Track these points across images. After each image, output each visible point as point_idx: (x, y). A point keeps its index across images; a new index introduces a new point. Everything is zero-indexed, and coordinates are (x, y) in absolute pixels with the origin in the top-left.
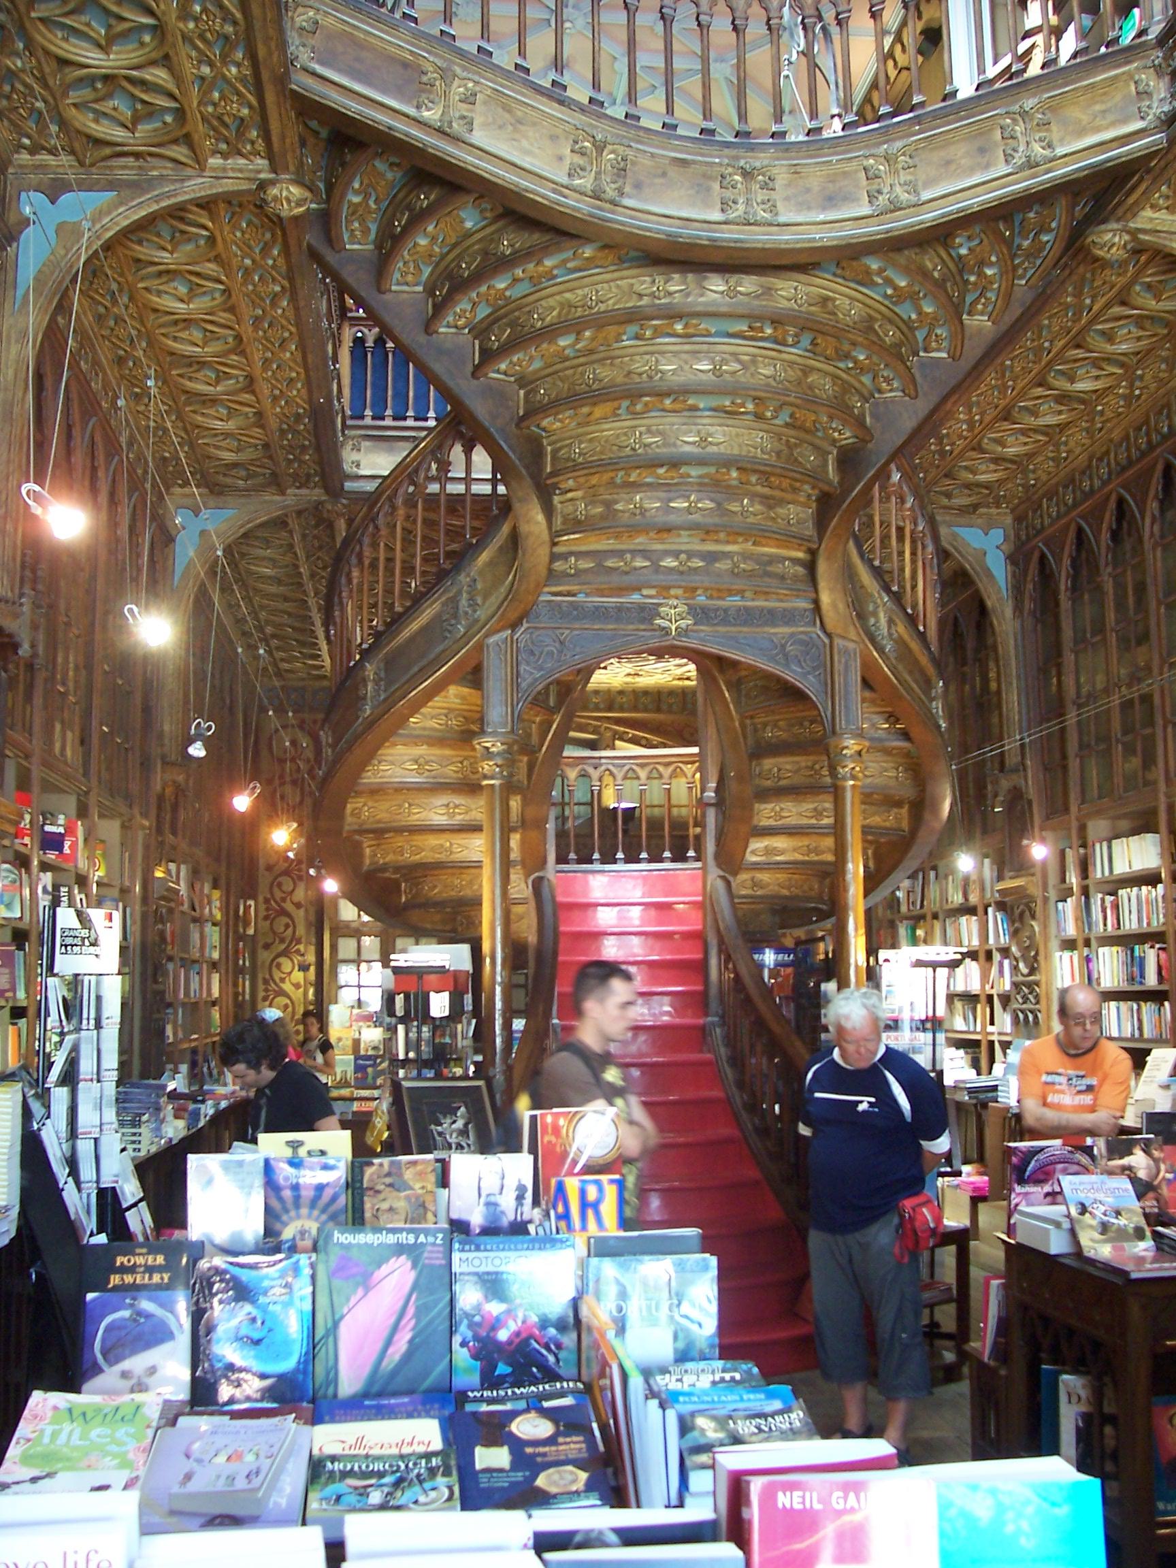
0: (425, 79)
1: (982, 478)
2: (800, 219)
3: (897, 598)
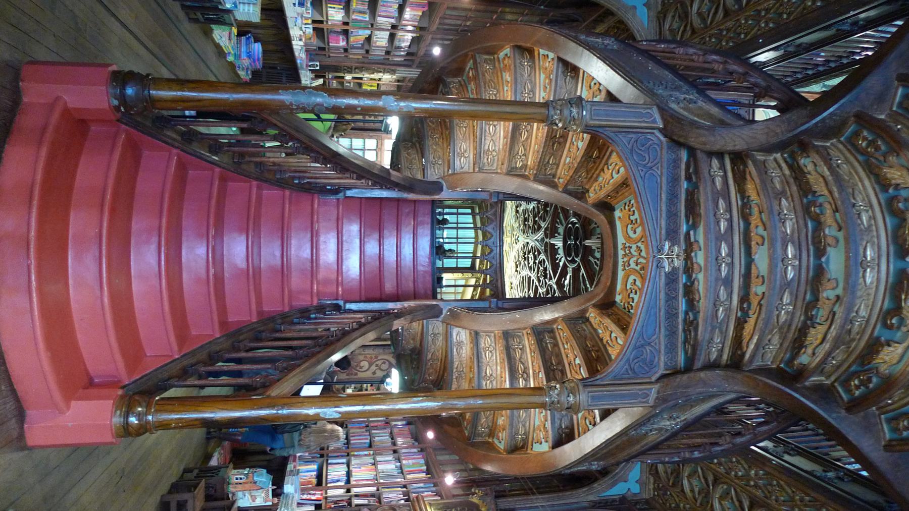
1: (685, 482)
3: (674, 435)
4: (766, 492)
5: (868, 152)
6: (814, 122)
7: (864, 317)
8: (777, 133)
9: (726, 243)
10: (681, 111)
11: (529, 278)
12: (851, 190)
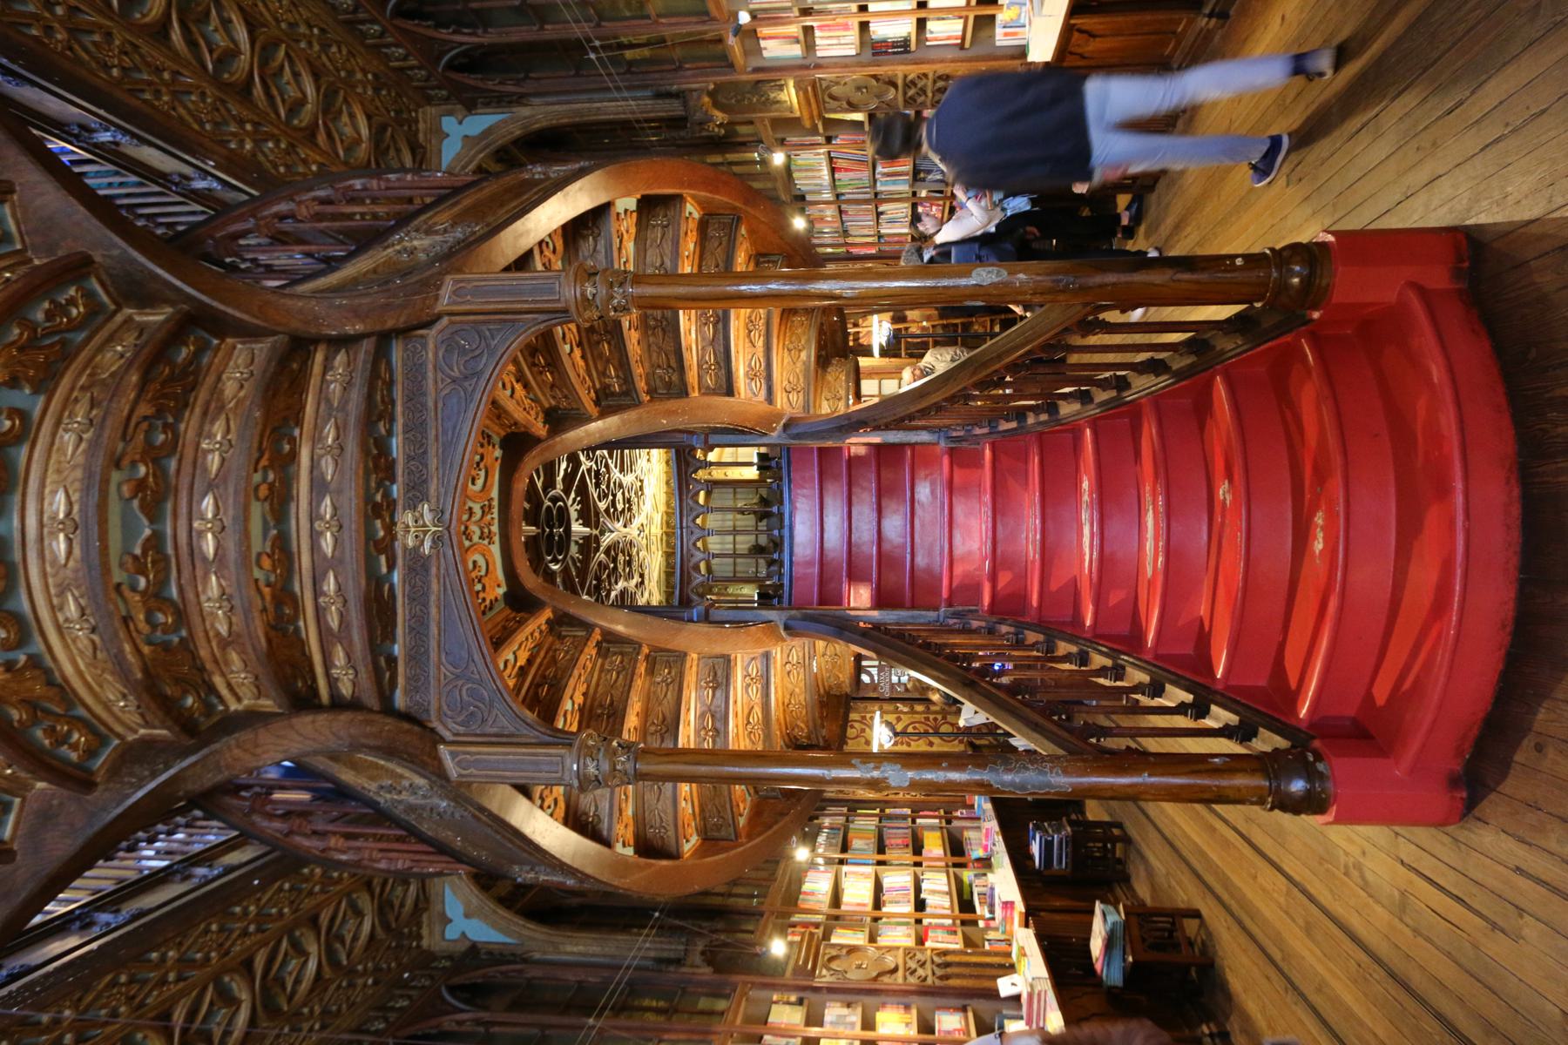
1: (365, 132)
3: (403, 221)
4: (222, 110)
5: (68, 723)
6: (172, 772)
7: (66, 431)
8: (238, 746)
9: (325, 555)
10: (407, 773)
11: (622, 470)
12: (99, 655)
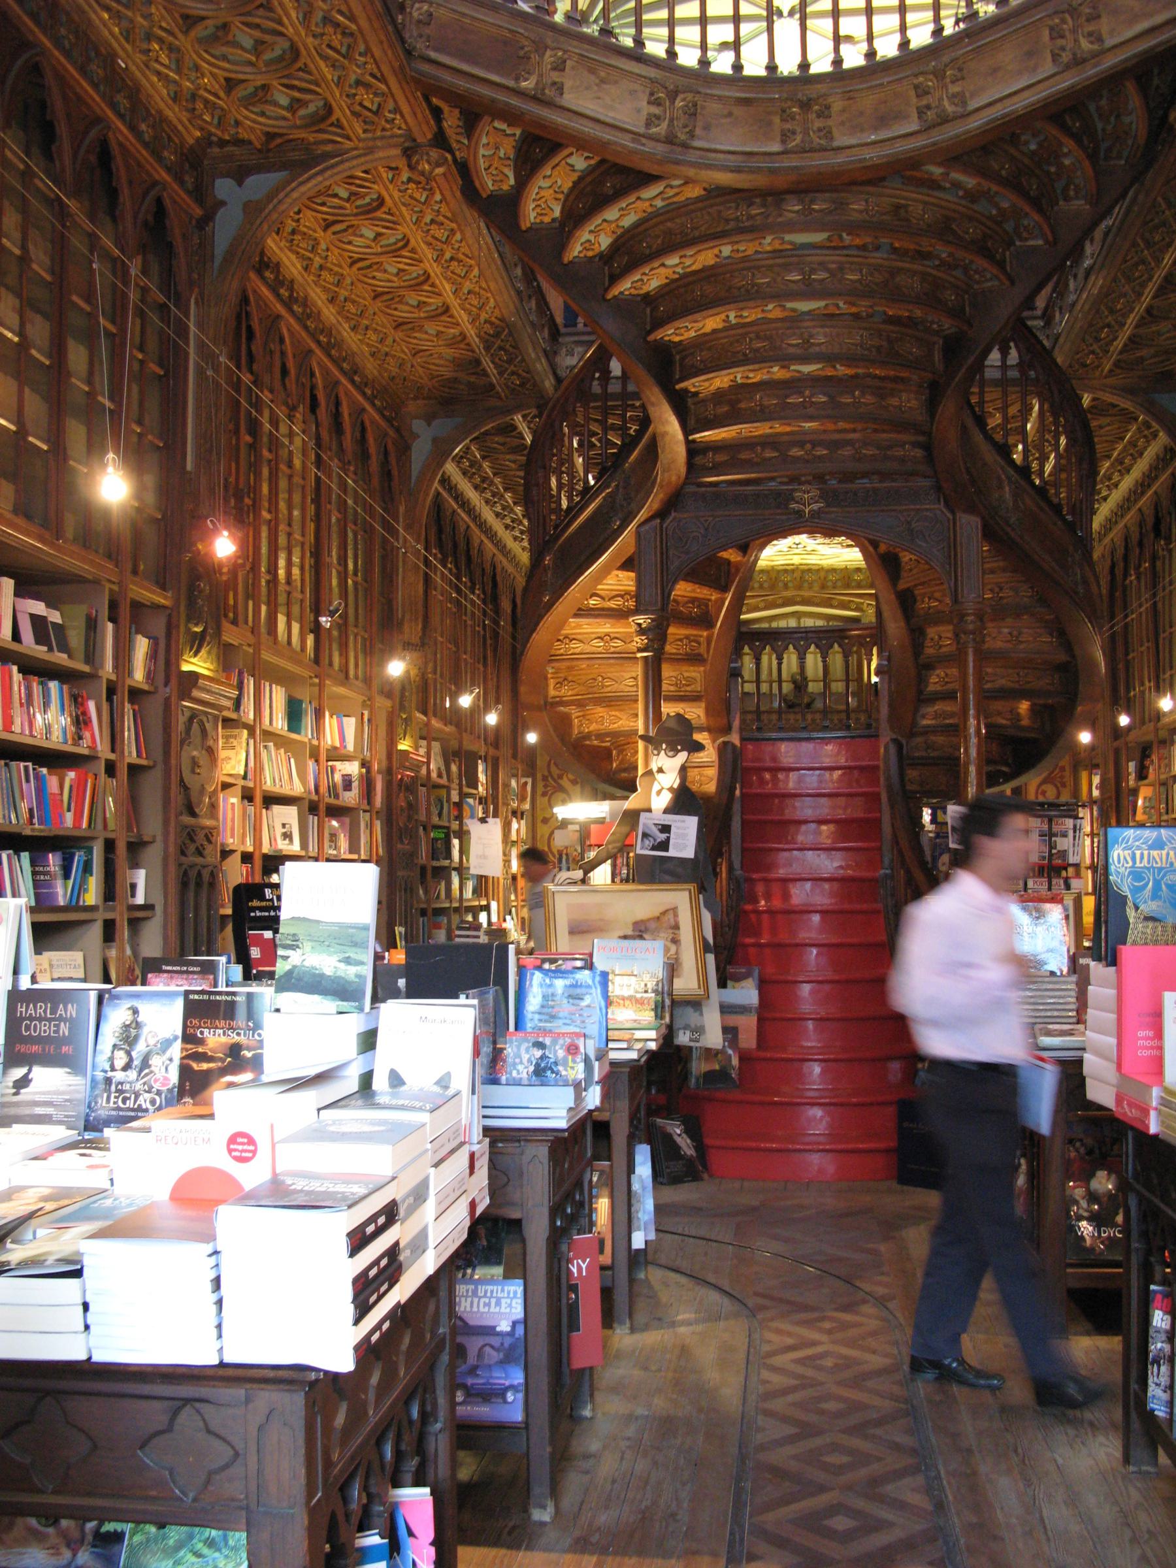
0: (521, 53)
2: (854, 141)
7: (862, 336)
